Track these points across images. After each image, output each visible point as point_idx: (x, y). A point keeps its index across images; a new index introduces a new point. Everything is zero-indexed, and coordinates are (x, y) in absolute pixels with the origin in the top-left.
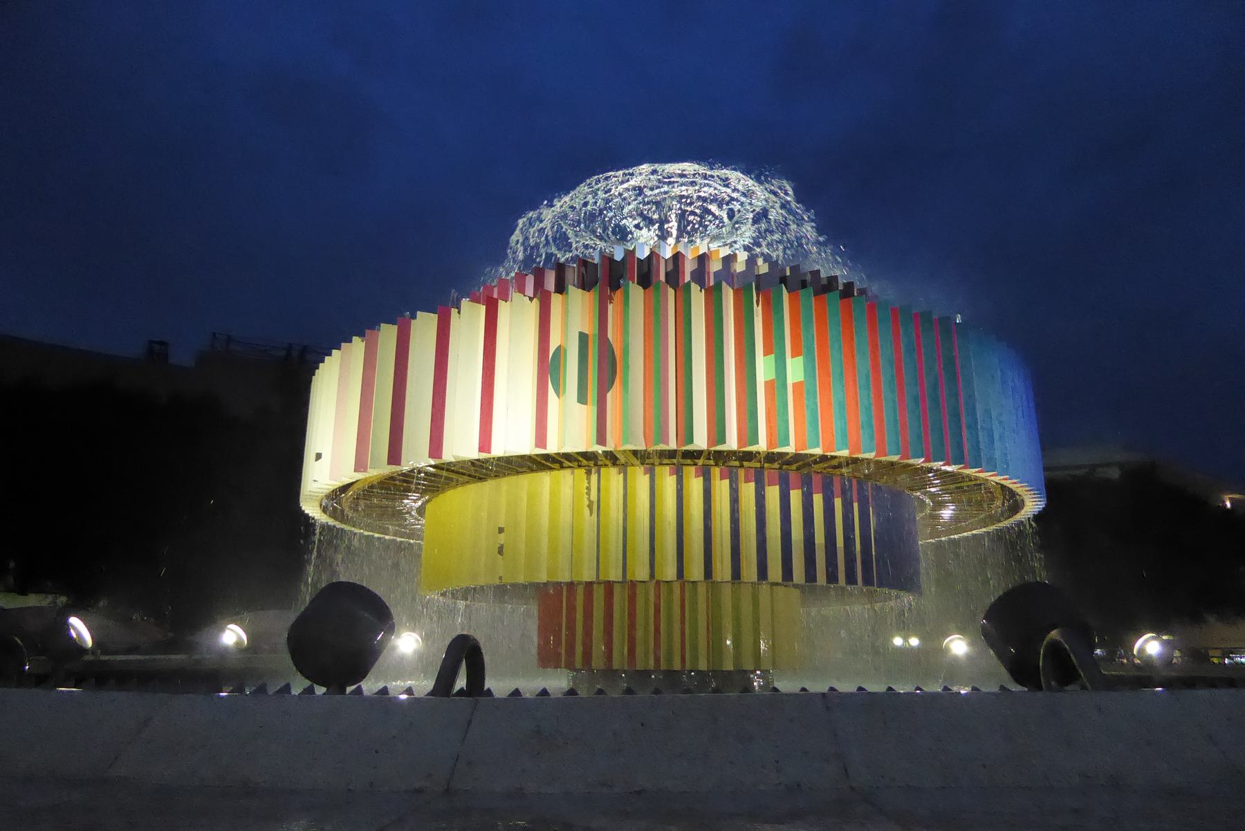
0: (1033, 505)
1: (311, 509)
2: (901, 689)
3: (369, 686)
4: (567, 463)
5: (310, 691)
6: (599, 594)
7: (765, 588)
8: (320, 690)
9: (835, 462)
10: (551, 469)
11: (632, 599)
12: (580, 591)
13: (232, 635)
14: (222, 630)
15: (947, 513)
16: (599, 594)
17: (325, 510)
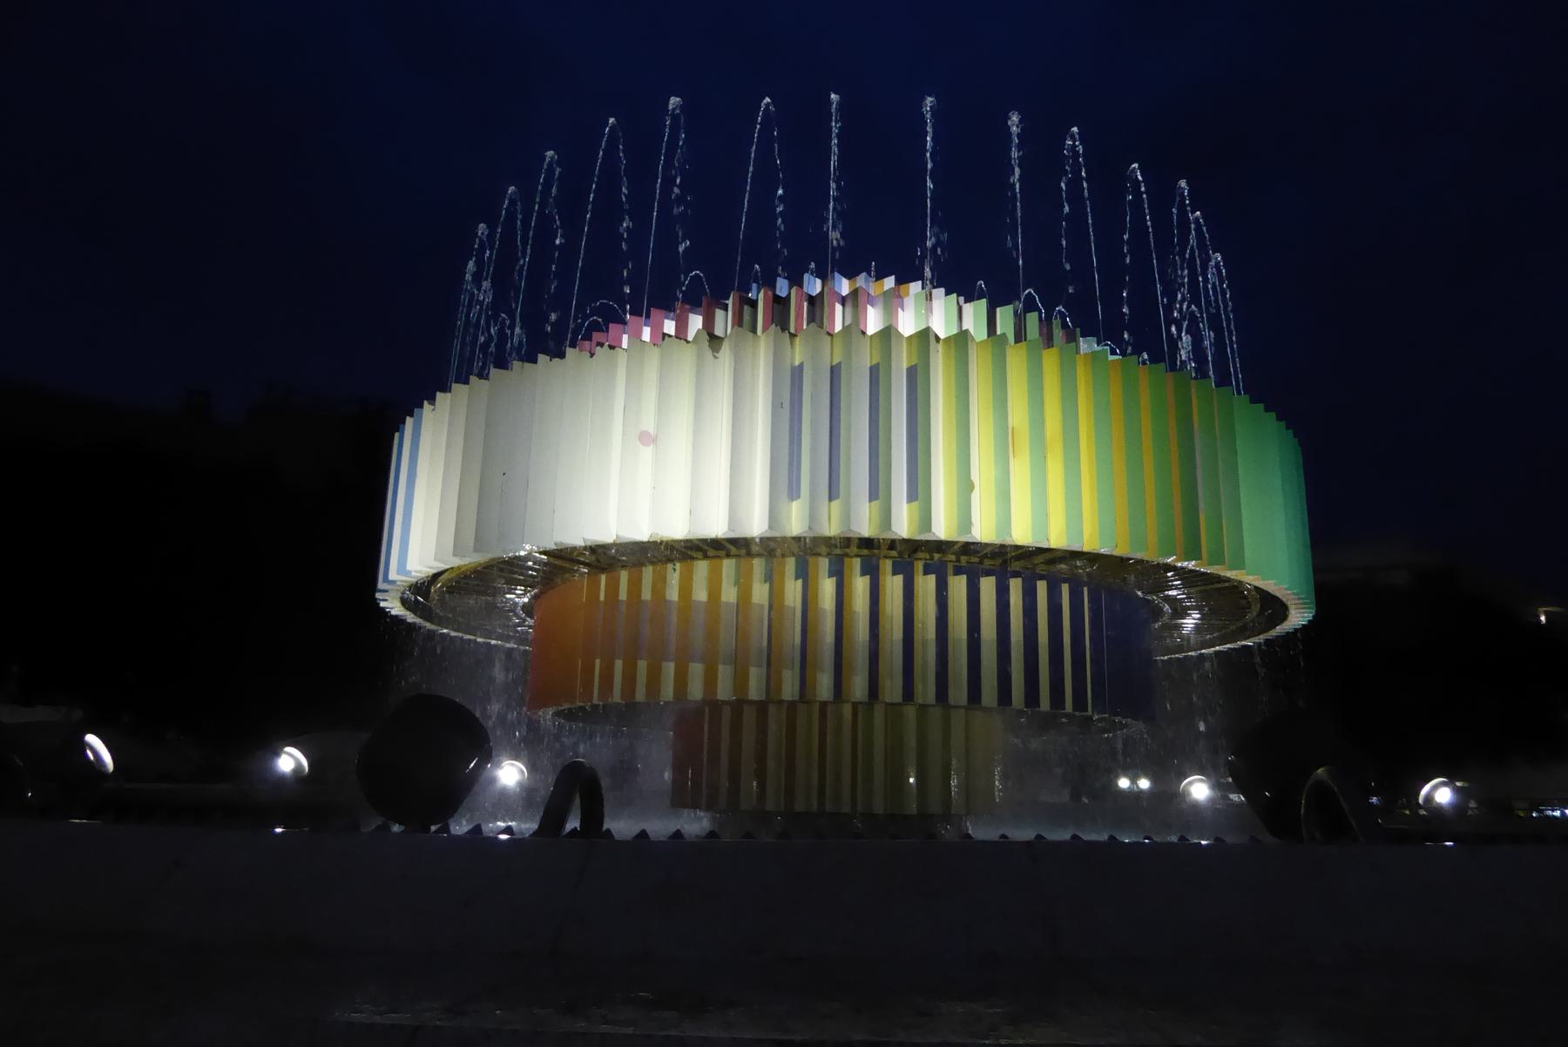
0: (1298, 617)
1: (393, 606)
2: (1086, 837)
3: (460, 827)
4: (711, 552)
5: (385, 828)
6: (749, 716)
7: (910, 712)
8: (396, 828)
9: (1048, 556)
10: (692, 558)
11: (736, 727)
12: (727, 713)
13: (290, 760)
14: (277, 754)
15: (1189, 623)
16: (749, 716)
17: (404, 602)
